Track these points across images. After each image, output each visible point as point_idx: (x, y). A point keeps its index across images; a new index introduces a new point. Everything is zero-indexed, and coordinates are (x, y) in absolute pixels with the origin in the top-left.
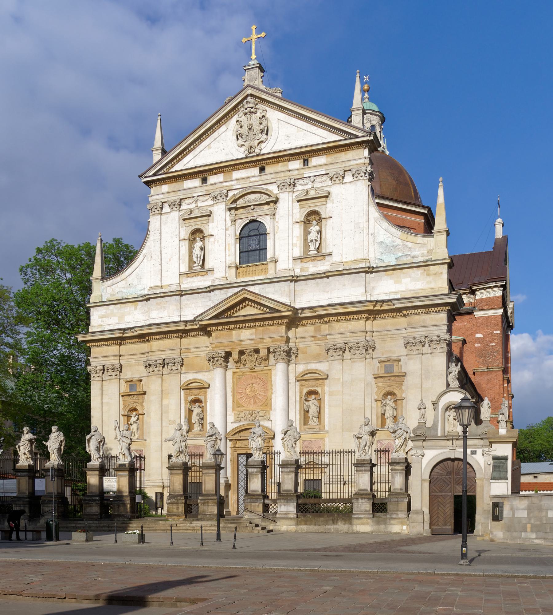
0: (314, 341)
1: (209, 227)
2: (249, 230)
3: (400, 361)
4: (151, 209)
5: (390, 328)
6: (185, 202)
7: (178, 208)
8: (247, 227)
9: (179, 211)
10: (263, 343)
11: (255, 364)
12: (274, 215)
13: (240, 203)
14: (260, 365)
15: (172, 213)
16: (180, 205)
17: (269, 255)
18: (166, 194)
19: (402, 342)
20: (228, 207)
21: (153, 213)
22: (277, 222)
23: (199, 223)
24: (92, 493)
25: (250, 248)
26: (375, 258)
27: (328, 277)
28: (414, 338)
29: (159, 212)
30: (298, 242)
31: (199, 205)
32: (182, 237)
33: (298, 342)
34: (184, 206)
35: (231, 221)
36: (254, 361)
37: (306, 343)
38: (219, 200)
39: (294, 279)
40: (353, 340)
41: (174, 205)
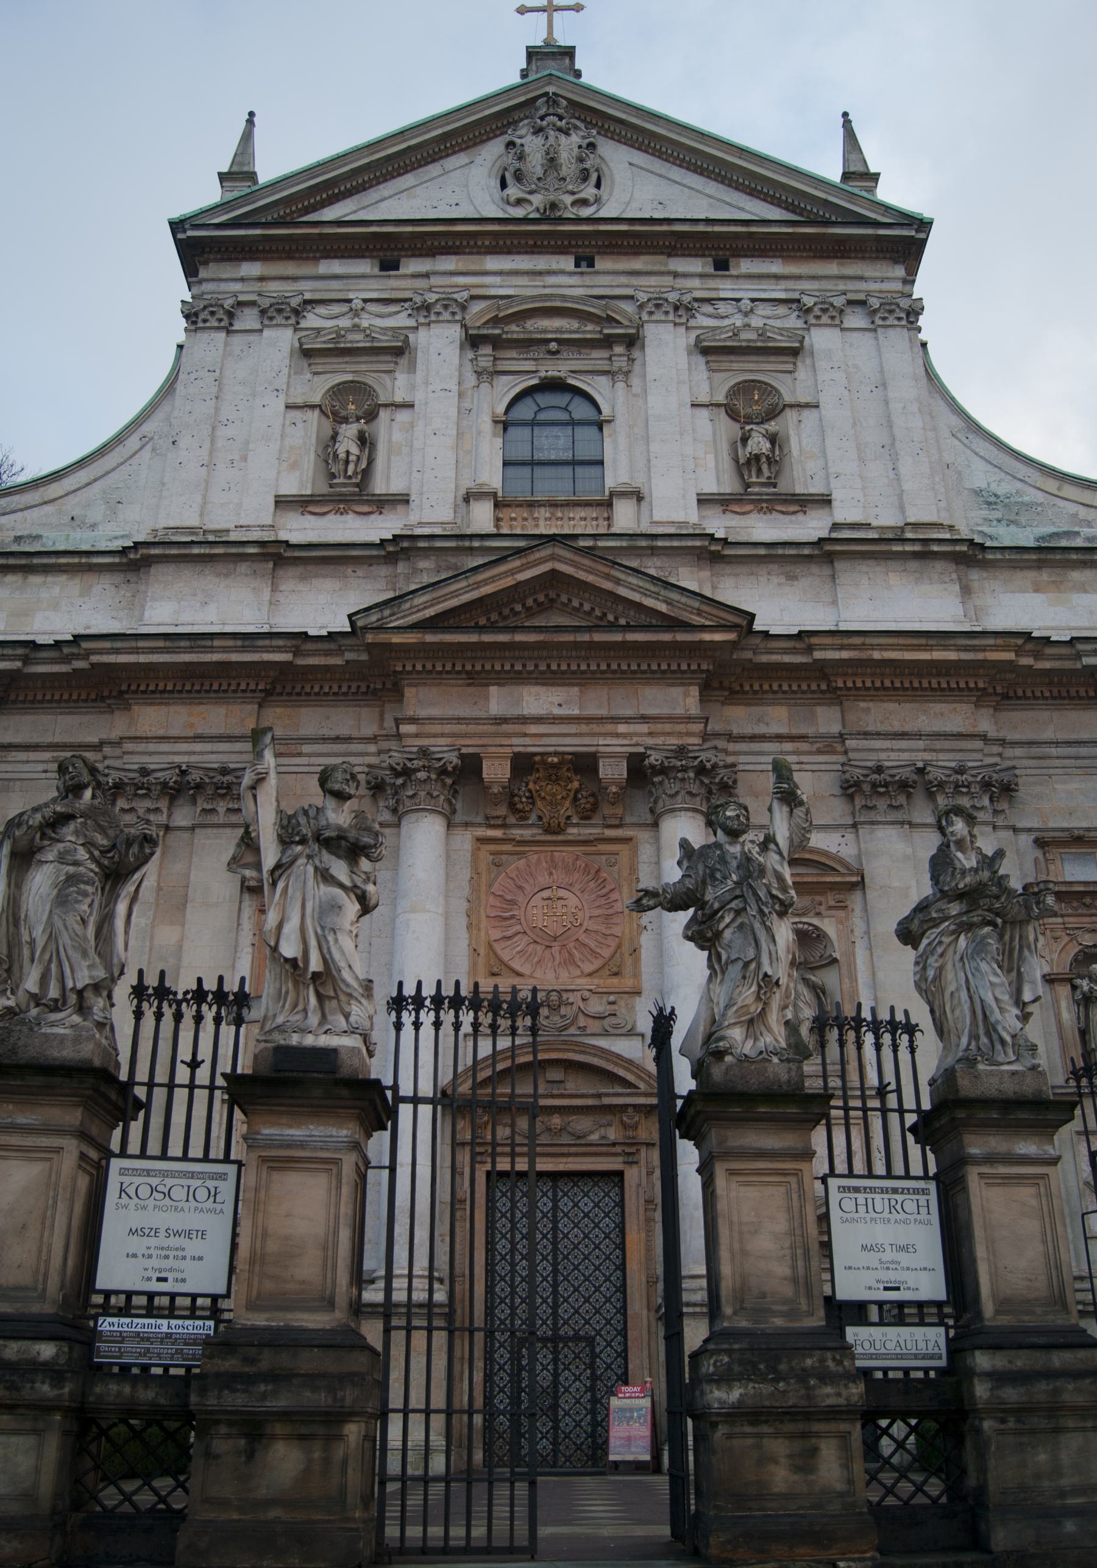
1: (397, 383)
2: (536, 409)
4: (196, 315)
5: (1048, 734)
6: (317, 311)
7: (292, 321)
8: (528, 401)
9: (296, 330)
10: (618, 735)
11: (569, 813)
12: (627, 373)
13: (514, 330)
14: (588, 818)
15: (266, 333)
16: (297, 312)
17: (615, 477)
18: (253, 283)
20: (470, 332)
21: (201, 325)
22: (635, 395)
23: (363, 367)
26: (972, 530)
29: (222, 324)
30: (711, 458)
31: (365, 324)
32: (299, 400)
33: (734, 753)
34: (312, 320)
35: (479, 374)
36: (567, 803)
38: (438, 314)
40: (944, 761)
41: (280, 311)
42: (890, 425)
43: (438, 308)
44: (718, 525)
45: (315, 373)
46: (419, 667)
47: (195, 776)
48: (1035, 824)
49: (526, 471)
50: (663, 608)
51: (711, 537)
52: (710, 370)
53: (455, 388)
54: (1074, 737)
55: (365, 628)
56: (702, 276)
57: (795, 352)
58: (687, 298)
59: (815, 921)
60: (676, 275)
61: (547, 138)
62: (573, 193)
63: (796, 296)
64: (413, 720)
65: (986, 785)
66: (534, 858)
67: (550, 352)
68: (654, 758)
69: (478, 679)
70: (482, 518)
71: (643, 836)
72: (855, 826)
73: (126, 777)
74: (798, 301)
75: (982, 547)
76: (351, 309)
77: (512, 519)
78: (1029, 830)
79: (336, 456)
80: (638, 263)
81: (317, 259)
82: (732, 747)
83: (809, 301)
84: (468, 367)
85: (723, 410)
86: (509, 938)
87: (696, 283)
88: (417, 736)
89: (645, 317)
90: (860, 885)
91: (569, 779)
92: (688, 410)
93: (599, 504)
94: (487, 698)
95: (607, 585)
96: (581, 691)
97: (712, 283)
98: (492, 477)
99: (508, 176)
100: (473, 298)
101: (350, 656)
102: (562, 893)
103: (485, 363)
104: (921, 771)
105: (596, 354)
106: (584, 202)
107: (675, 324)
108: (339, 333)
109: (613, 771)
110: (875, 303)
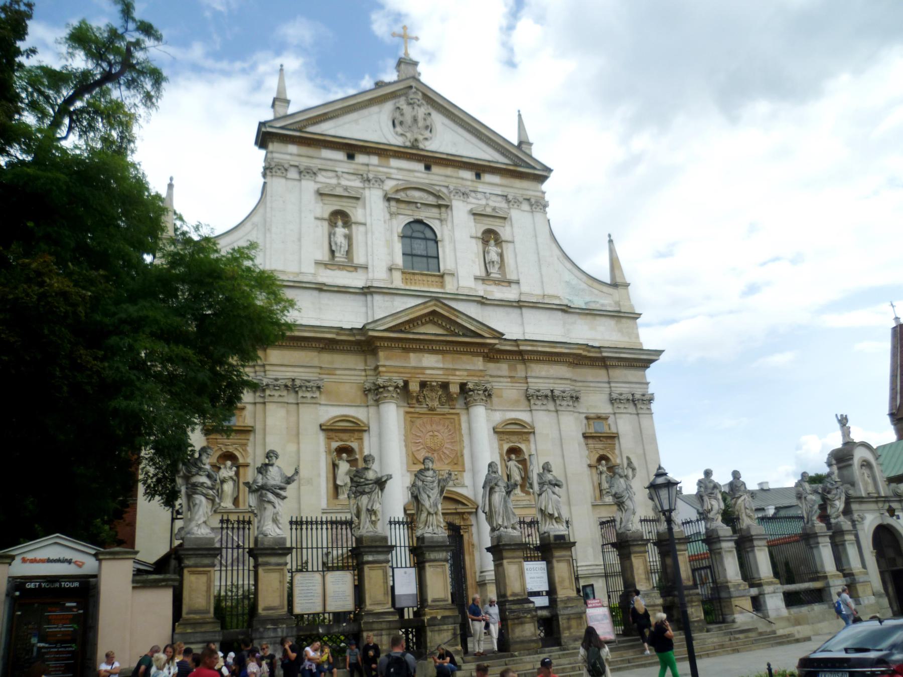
0: (511, 382)
3: (606, 419)
4: (272, 169)
9: (316, 182)
12: (446, 220)
13: (401, 196)
15: (304, 182)
19: (605, 397)
21: (274, 174)
23: (344, 204)
24: (514, 594)
25: (414, 252)
27: (520, 307)
28: (621, 394)
30: (477, 260)
31: (344, 182)
32: (319, 215)
34: (321, 178)
35: (391, 214)
36: (437, 400)
37: (500, 384)
39: (483, 301)
40: (558, 387)
41: (308, 173)
42: (538, 254)
43: (373, 181)
44: (481, 290)
45: (325, 204)
46: (386, 345)
47: (298, 383)
48: (585, 411)
49: (410, 258)
50: (473, 328)
51: (482, 297)
52: (475, 222)
53: (382, 219)
54: (597, 380)
55: (369, 330)
56: (472, 181)
57: (505, 218)
58: (467, 191)
59: (519, 445)
60: (463, 179)
61: (413, 108)
62: (422, 135)
63: (505, 194)
64: (384, 366)
65: (572, 397)
66: (425, 420)
67: (417, 208)
68: (470, 386)
69: (407, 350)
70: (398, 281)
71: (463, 413)
72: (531, 411)
73: (270, 382)
74: (506, 196)
75: (570, 307)
76: (337, 176)
77: (407, 279)
78: (583, 413)
79: (336, 244)
80: (449, 171)
81: (320, 148)
82: (491, 379)
83: (510, 197)
84: (386, 210)
85: (480, 241)
86: (418, 450)
87: (469, 183)
88: (386, 372)
89: (452, 197)
90: (534, 433)
91: (438, 391)
92: (469, 239)
93: (438, 276)
94: (409, 358)
95: (453, 318)
96: (443, 358)
97: (475, 184)
98: (399, 260)
99: (396, 122)
100: (388, 178)
101: (358, 338)
102: (436, 433)
103: (393, 209)
104: (552, 391)
105: (435, 210)
106: (426, 139)
107: (463, 201)
108: (334, 187)
109: (454, 389)
110: (533, 201)
